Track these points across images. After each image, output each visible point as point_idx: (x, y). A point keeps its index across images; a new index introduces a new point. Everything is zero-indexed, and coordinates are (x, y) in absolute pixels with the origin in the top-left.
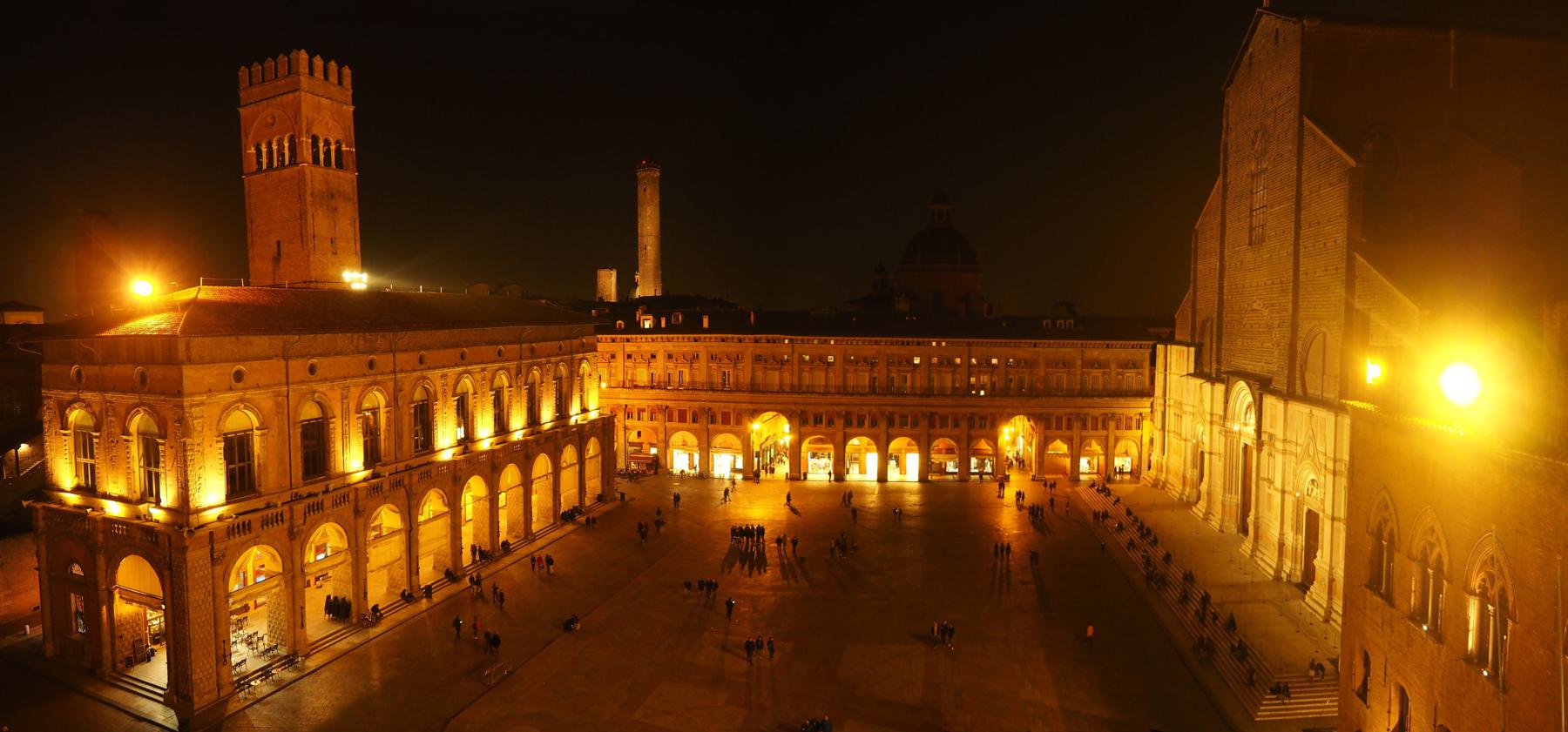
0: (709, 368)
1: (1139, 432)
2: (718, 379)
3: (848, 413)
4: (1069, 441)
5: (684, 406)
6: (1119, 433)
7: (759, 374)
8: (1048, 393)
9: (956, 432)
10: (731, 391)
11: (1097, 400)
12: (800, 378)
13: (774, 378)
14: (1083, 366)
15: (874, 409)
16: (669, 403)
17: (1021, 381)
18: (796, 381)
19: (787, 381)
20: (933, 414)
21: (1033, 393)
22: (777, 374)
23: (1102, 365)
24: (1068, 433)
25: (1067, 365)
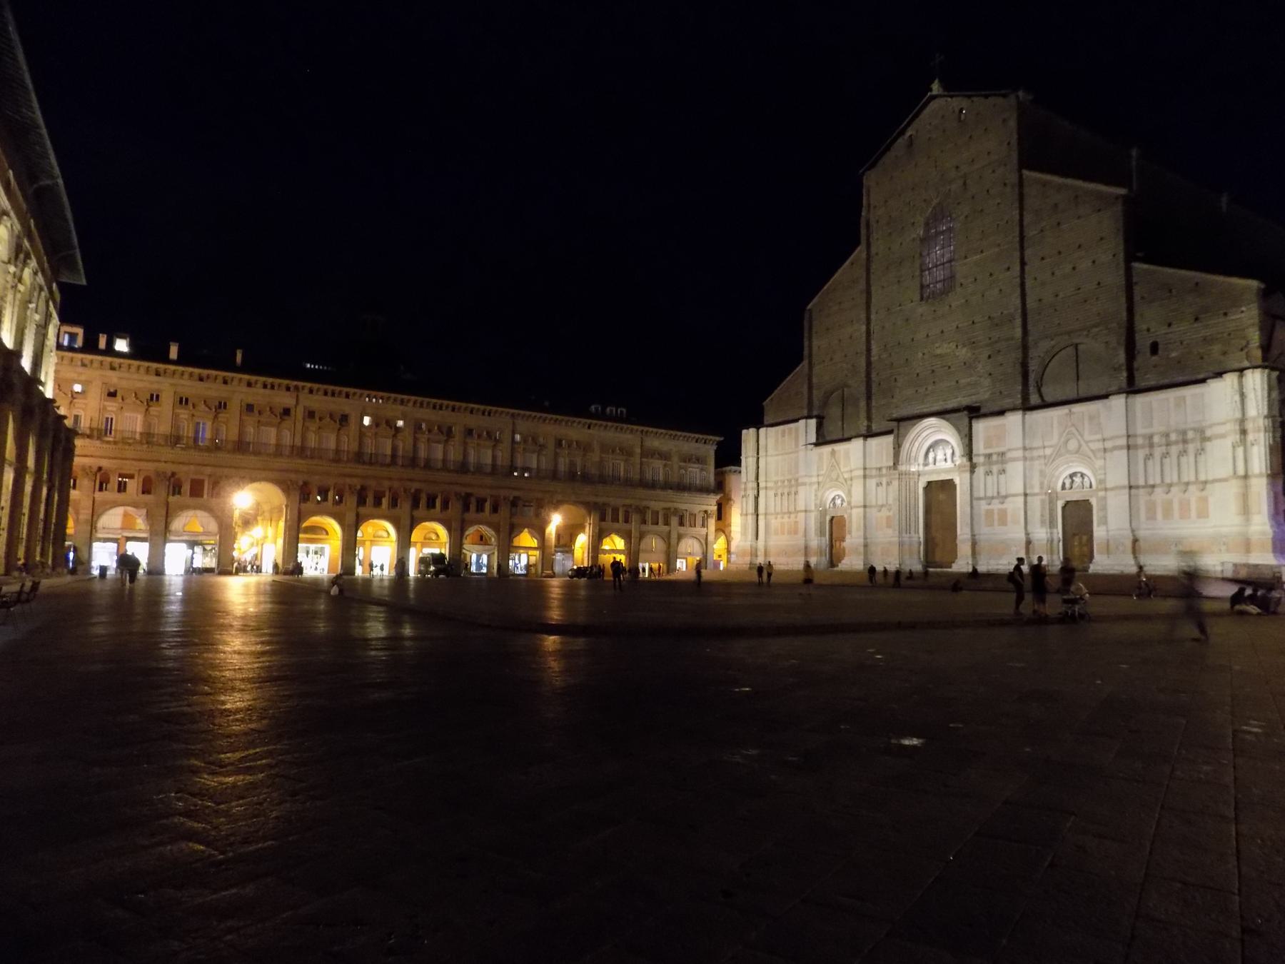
0: (175, 417)
1: (704, 531)
2: (187, 431)
3: (363, 488)
4: (627, 536)
5: (129, 467)
6: (682, 530)
7: (250, 430)
8: (603, 480)
9: (495, 518)
10: (208, 449)
11: (659, 492)
12: (304, 438)
13: (270, 435)
14: (643, 455)
15: (396, 484)
16: (105, 463)
17: (572, 464)
18: (298, 442)
19: (287, 439)
20: (469, 495)
21: (586, 479)
22: (273, 431)
23: (665, 456)
24: (626, 526)
25: (627, 452)
